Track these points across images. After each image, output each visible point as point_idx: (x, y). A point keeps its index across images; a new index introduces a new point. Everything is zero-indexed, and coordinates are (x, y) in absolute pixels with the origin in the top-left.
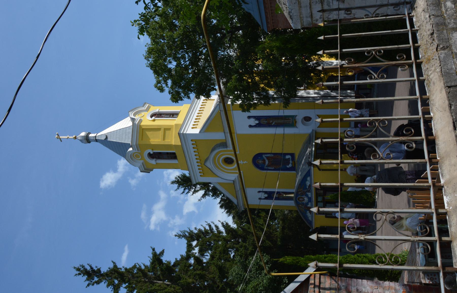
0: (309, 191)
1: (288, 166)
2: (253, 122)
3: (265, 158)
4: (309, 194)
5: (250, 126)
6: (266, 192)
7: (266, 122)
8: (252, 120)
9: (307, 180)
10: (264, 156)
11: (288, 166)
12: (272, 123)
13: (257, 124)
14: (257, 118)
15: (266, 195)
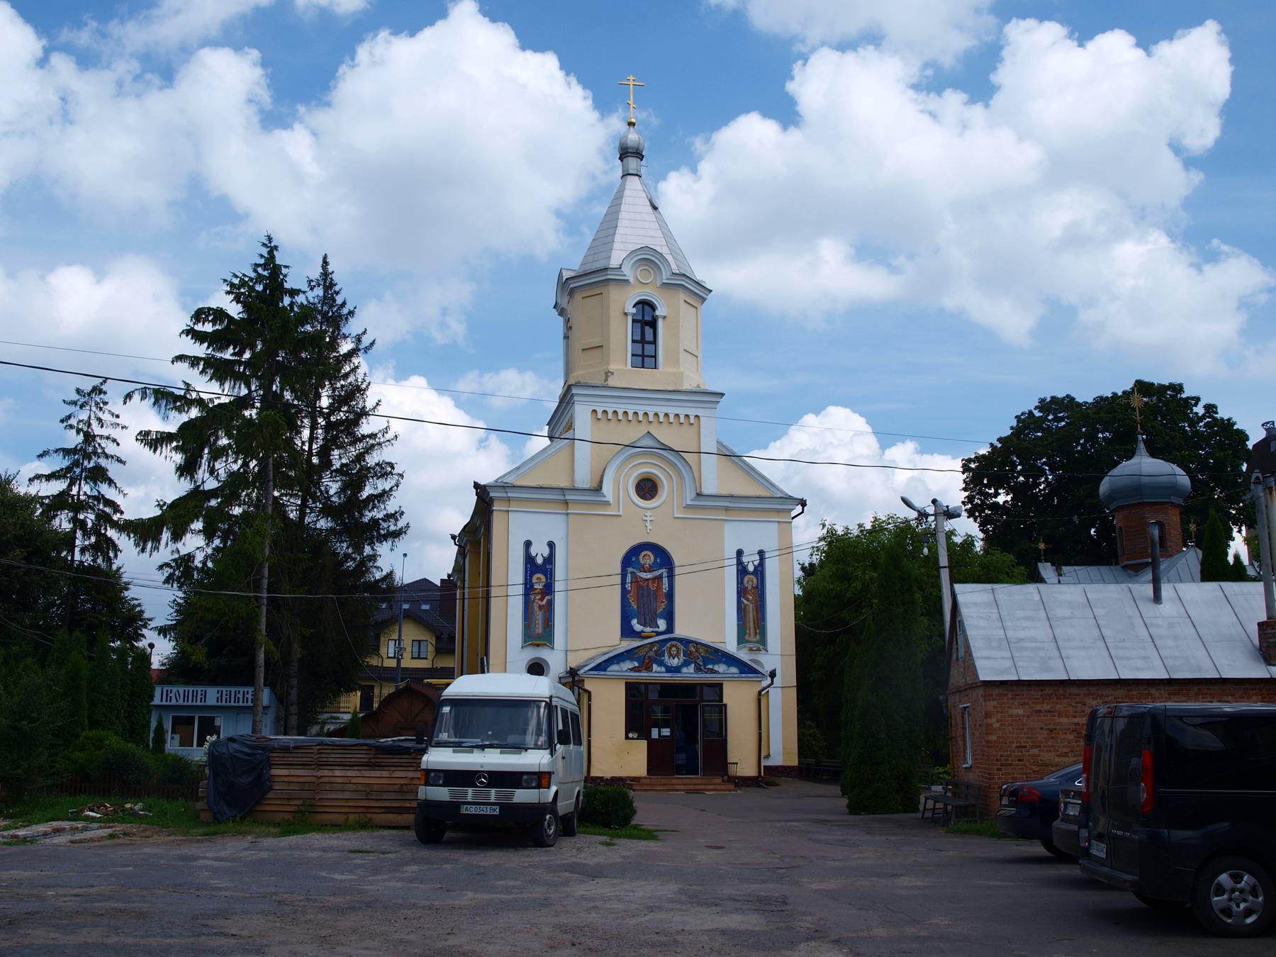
0: (698, 669)
1: (634, 622)
2: (751, 561)
3: (657, 573)
4: (691, 668)
6: (550, 560)
9: (729, 665)
10: (664, 571)
11: (634, 622)
12: (747, 599)
14: (760, 571)
15: (540, 560)
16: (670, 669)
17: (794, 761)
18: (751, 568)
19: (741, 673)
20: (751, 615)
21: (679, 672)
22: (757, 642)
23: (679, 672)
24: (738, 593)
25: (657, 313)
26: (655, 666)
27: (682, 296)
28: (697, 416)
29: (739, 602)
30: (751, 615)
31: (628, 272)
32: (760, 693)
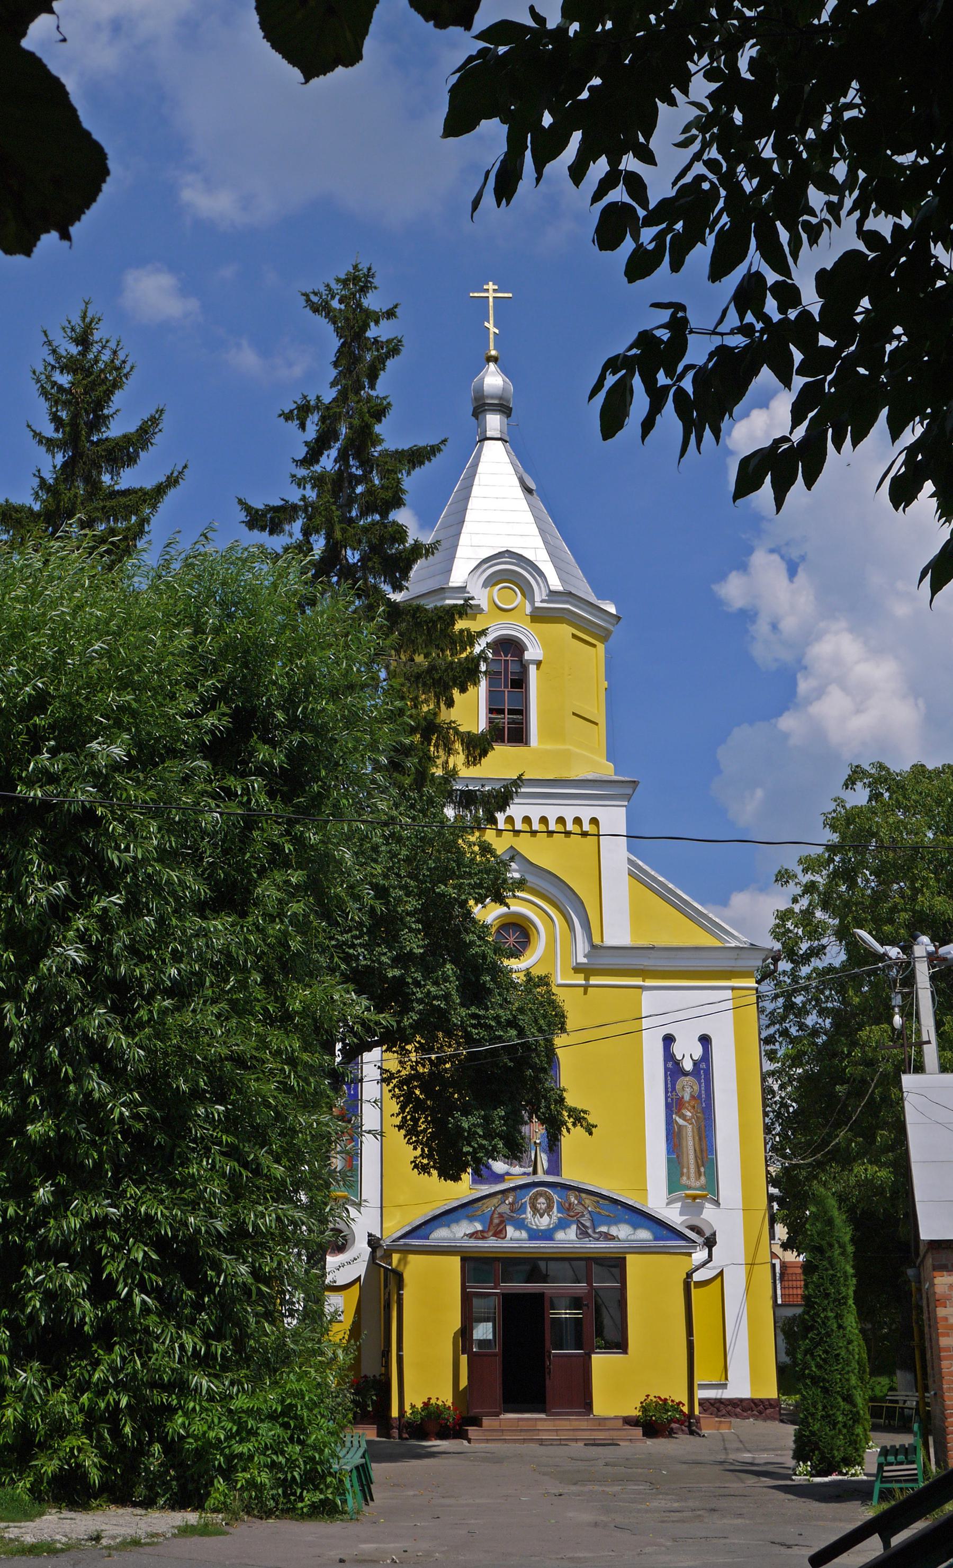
0: (583, 1233)
2: (687, 1051)
5: (669, 1040)
7: (687, 1097)
8: (697, 1051)
9: (635, 1227)
12: (684, 1117)
13: (677, 1063)
14: (703, 1068)
16: (535, 1235)
17: (770, 1391)
18: (688, 1066)
19: (656, 1239)
20: (690, 1143)
21: (552, 1239)
22: (702, 1188)
23: (552, 1239)
24: (668, 1106)
25: (527, 656)
26: (510, 1231)
27: (566, 630)
28: (594, 821)
29: (669, 1122)
30: (690, 1143)
31: (481, 597)
32: (689, 1275)
